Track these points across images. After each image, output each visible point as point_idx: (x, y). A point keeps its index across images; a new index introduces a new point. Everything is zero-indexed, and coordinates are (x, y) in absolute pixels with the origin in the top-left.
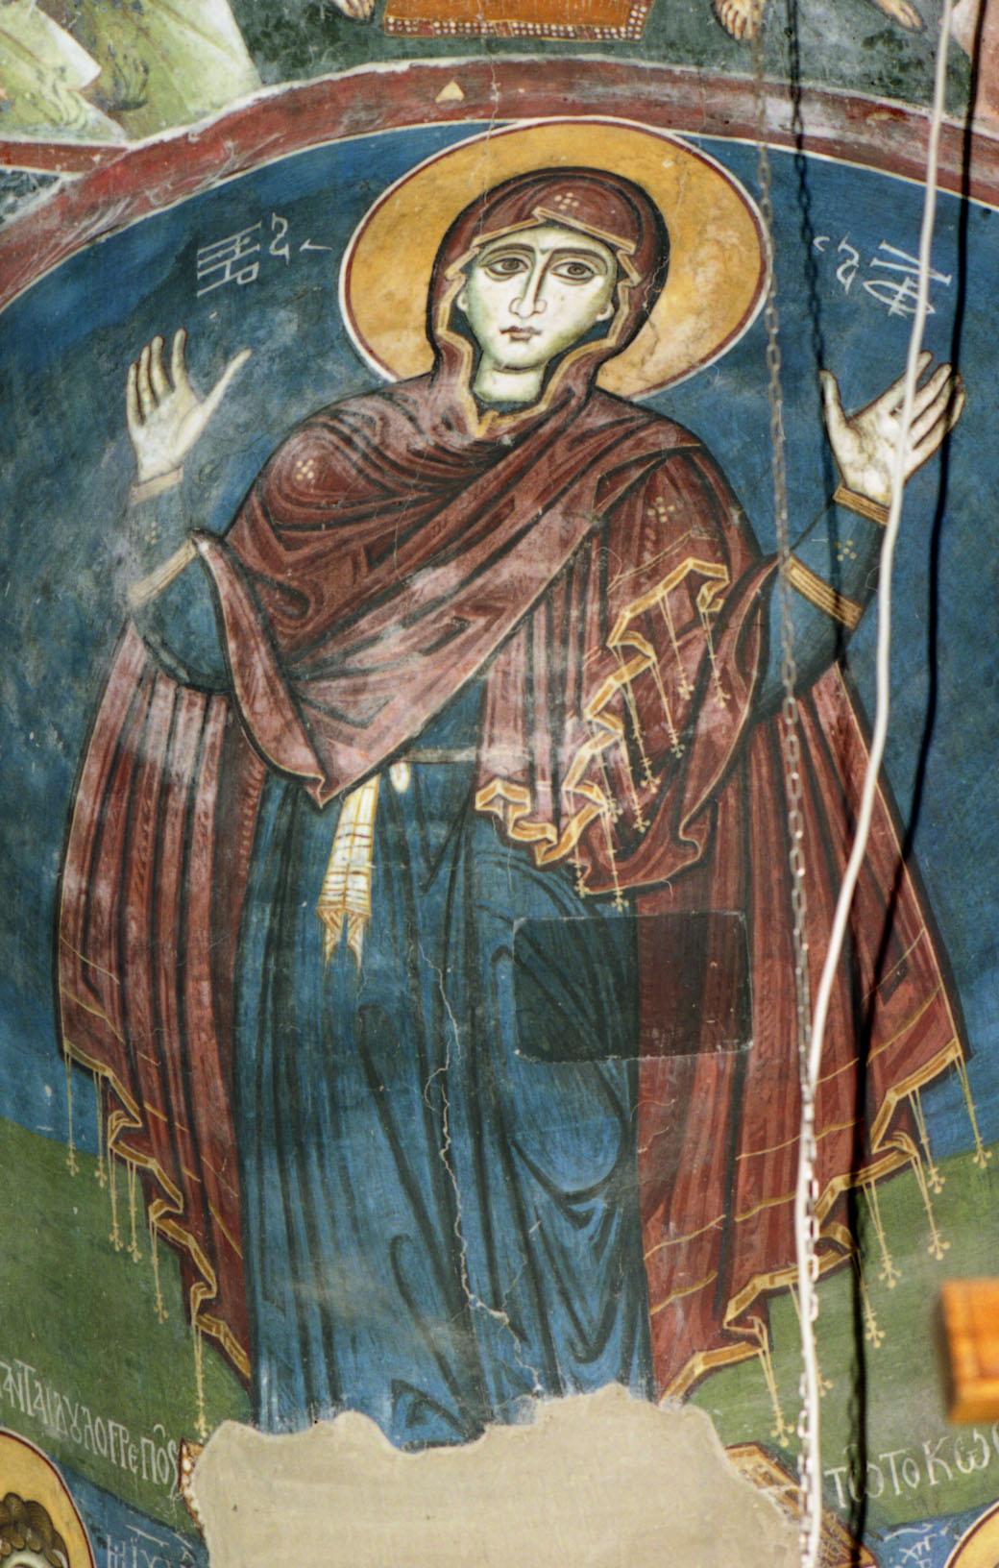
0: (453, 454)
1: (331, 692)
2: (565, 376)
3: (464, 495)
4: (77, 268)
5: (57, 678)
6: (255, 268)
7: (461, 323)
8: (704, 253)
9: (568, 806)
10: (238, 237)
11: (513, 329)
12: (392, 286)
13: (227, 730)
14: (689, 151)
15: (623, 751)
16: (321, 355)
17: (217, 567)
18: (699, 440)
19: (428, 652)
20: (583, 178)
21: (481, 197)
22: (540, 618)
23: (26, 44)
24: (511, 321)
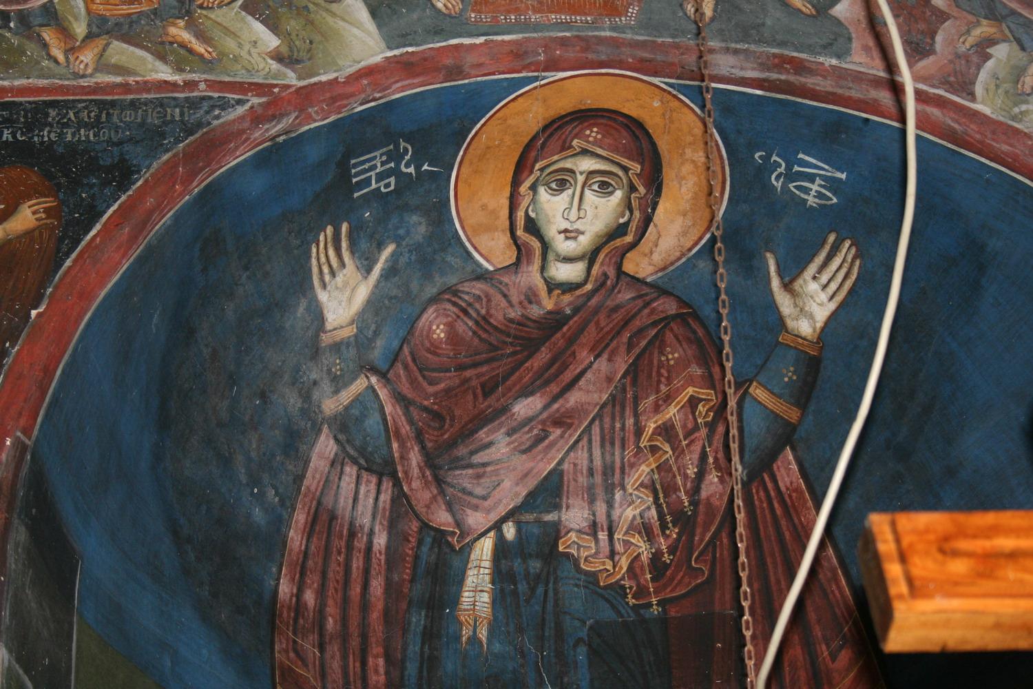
0: (535, 321)
1: (462, 478)
2: (602, 264)
3: (543, 349)
4: (263, 160)
5: (273, 456)
6: (392, 180)
7: (532, 227)
8: (687, 169)
9: (619, 547)
10: (377, 153)
11: (566, 231)
12: (485, 200)
13: (393, 500)
14: (669, 93)
15: (653, 512)
16: (443, 250)
17: (383, 394)
18: (690, 307)
19: (524, 452)
20: (603, 117)
21: (538, 133)
22: (596, 430)
23: (232, 29)
24: (565, 225)
